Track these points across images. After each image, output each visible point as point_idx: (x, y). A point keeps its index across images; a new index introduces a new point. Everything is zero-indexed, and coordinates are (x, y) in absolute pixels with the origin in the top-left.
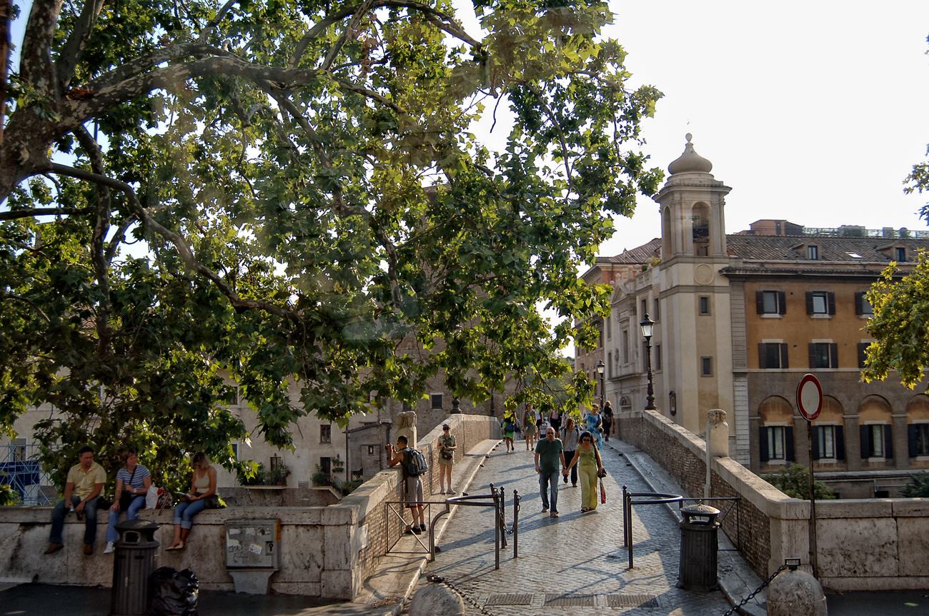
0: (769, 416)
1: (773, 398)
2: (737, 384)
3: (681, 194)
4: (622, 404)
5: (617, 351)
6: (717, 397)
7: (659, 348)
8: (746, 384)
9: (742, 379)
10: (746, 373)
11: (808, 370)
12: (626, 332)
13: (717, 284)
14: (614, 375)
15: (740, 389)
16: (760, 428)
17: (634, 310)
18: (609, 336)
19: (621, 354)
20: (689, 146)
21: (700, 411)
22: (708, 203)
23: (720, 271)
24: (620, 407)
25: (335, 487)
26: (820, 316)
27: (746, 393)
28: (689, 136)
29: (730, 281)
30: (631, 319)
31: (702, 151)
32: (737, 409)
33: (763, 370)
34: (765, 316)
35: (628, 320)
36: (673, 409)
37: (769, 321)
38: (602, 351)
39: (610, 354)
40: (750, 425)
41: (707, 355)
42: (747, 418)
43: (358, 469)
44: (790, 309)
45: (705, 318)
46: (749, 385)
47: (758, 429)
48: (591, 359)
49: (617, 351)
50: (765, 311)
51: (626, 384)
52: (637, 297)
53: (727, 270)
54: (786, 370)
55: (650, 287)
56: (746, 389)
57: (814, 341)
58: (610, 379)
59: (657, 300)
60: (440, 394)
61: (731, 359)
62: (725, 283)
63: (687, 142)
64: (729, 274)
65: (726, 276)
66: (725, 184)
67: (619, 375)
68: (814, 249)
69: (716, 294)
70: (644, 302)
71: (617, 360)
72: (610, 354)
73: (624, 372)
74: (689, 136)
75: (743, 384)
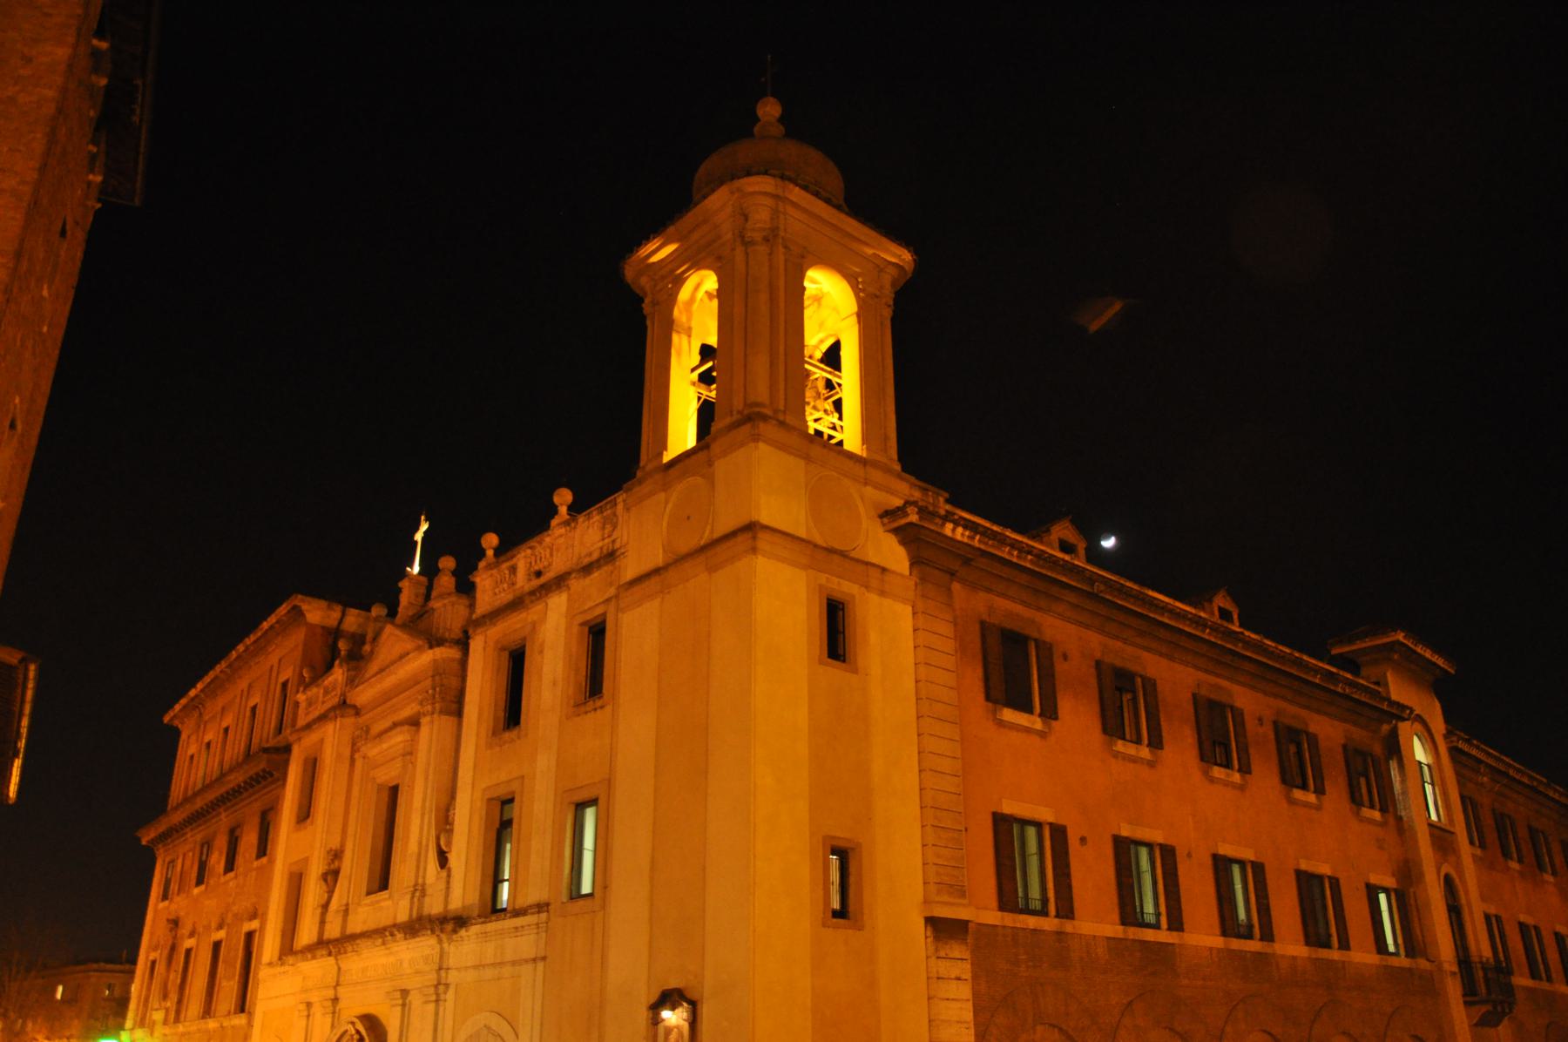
2: (943, 968)
8: (965, 970)
9: (957, 950)
18: (305, 814)
26: (1131, 749)
27: (969, 1015)
37: (1014, 737)
44: (1065, 705)
46: (975, 977)
48: (211, 905)
52: (476, 645)
54: (1069, 926)
56: (965, 991)
75: (958, 963)
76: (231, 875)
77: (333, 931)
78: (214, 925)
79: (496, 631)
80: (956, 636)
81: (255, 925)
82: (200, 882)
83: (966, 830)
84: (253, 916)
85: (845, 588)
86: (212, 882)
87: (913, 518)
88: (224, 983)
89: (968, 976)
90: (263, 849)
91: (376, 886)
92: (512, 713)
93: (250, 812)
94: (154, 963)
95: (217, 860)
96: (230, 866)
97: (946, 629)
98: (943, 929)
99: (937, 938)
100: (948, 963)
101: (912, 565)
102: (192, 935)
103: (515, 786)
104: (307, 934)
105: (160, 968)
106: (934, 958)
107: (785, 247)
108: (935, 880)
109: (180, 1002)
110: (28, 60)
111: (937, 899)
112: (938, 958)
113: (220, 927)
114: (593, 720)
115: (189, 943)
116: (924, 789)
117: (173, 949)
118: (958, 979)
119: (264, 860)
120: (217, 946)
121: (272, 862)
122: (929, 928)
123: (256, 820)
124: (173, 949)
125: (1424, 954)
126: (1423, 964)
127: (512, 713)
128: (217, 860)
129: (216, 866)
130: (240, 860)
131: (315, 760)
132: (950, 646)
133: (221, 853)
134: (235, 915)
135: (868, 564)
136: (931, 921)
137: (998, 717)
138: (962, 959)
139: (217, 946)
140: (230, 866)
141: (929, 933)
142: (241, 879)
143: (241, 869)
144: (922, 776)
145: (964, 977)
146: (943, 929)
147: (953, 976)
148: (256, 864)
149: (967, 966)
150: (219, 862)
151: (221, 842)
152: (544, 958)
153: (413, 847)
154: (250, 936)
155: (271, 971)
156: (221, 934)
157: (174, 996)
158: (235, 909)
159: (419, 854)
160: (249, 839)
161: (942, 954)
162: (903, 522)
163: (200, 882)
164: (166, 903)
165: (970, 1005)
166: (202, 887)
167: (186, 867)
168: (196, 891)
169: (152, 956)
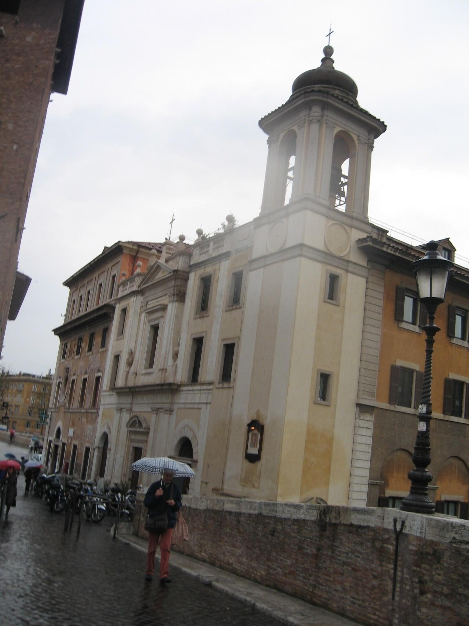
0: (392, 481)
1: (399, 453)
2: (361, 423)
3: (323, 110)
4: (131, 426)
5: (131, 354)
6: (330, 441)
8: (371, 425)
9: (368, 417)
10: (372, 408)
12: (155, 329)
14: (120, 383)
15: (364, 432)
16: (380, 498)
17: (181, 297)
18: (121, 332)
19: (141, 357)
21: (306, 460)
22: (355, 138)
23: (360, 241)
24: (124, 430)
27: (370, 441)
28: (328, 51)
29: (369, 261)
30: (172, 308)
32: (358, 464)
33: (392, 408)
35: (164, 308)
36: (254, 451)
38: (104, 354)
40: (369, 492)
41: (326, 369)
42: (366, 481)
46: (375, 427)
47: (378, 498)
48: (82, 363)
49: (131, 354)
50: (405, 319)
51: (139, 399)
52: (192, 276)
55: (227, 255)
56: (370, 433)
58: (113, 388)
61: (355, 383)
67: (131, 384)
68: (447, 253)
69: (350, 275)
71: (130, 364)
73: (143, 380)
74: (328, 51)
76: (90, 353)
78: (83, 373)
79: (201, 272)
80: (384, 292)
81: (100, 374)
82: (78, 353)
83: (379, 371)
84: (99, 371)
85: (338, 271)
86: (83, 355)
87: (370, 243)
88: (87, 395)
89: (372, 427)
90: (104, 344)
91: (148, 366)
93: (98, 331)
94: (59, 383)
95: (85, 346)
96: (90, 349)
97: (382, 289)
98: (362, 408)
99: (360, 412)
100: (364, 422)
101: (368, 262)
102: (74, 374)
103: (204, 335)
105: (62, 385)
106: (358, 419)
107: (326, 123)
108: (362, 390)
109: (70, 400)
110: (37, 67)
111: (363, 397)
112: (360, 419)
113: (85, 373)
114: (236, 313)
115: (74, 377)
116: (363, 353)
117: (67, 379)
118: (367, 428)
119: (104, 349)
120: (85, 380)
121: (107, 350)
122: (357, 407)
123: (101, 332)
124: (67, 379)
128: (85, 346)
129: (84, 349)
130: (94, 347)
132: (381, 296)
133: (86, 345)
134: (92, 370)
135: (348, 262)
137: (399, 326)
138: (370, 421)
139: (85, 380)
140: (90, 349)
141: (357, 410)
142: (94, 355)
143: (94, 351)
144: (362, 348)
145: (370, 427)
146: (362, 408)
147: (365, 427)
148: (101, 350)
149: (372, 424)
150: (86, 347)
151: (86, 339)
152: (210, 403)
153: (163, 351)
154: (98, 379)
156: (86, 376)
157: (68, 398)
158: (92, 367)
159: (165, 356)
160: (98, 340)
161: (362, 418)
162: (365, 244)
163: (78, 353)
164: (64, 360)
165: (371, 438)
166: (79, 356)
167: (72, 347)
168: (76, 357)
169: (59, 380)
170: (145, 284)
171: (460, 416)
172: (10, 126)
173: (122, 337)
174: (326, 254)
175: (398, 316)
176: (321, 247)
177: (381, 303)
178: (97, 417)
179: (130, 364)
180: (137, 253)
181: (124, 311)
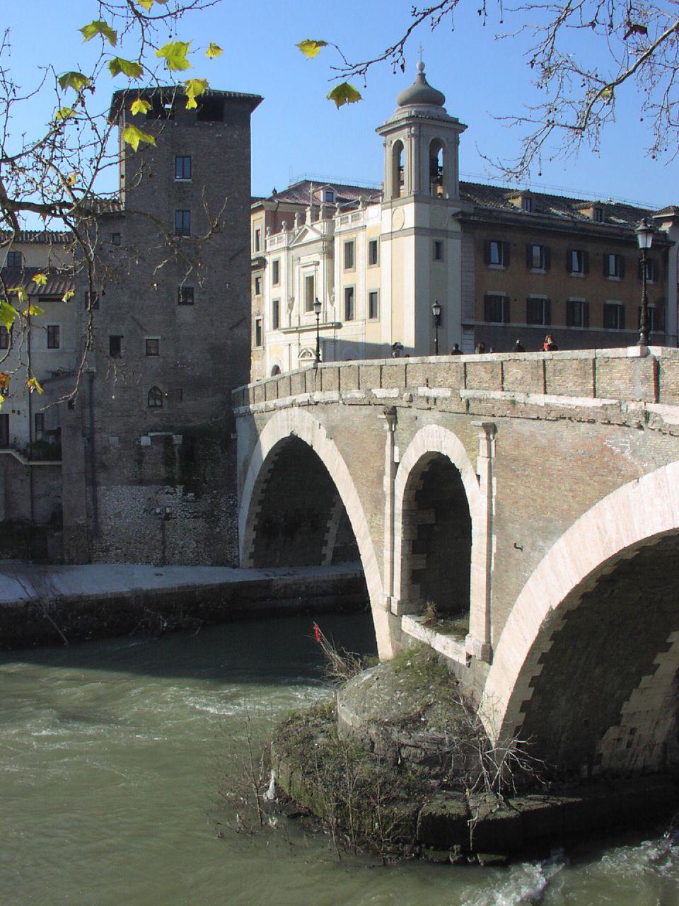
2: (466, 337)
7: (373, 297)
8: (472, 337)
9: (469, 332)
10: (473, 326)
11: (525, 325)
13: (450, 228)
18: (276, 280)
20: (422, 76)
23: (455, 215)
25: (18, 450)
26: (537, 271)
31: (435, 83)
33: (487, 324)
34: (492, 266)
39: (276, 305)
43: (55, 428)
45: (438, 264)
53: (462, 213)
54: (508, 325)
57: (532, 296)
59: (374, 246)
60: (156, 338)
62: (456, 227)
63: (419, 72)
64: (464, 220)
65: (460, 221)
66: (460, 121)
70: (349, 247)
71: (290, 307)
72: (276, 305)
77: (295, 323)
92: (349, 262)
98: (466, 327)
104: (284, 323)
114: (375, 269)
119: (260, 296)
125: (664, 329)
126: (662, 333)
127: (349, 262)
131: (277, 262)
136: (463, 325)
155: (269, 333)
170: (296, 242)
171: (541, 324)
172: (236, 195)
173: (278, 284)
174: (432, 230)
175: (487, 260)
176: (428, 226)
177: (472, 254)
178: (264, 354)
179: (290, 307)
180: (277, 208)
181: (276, 264)
